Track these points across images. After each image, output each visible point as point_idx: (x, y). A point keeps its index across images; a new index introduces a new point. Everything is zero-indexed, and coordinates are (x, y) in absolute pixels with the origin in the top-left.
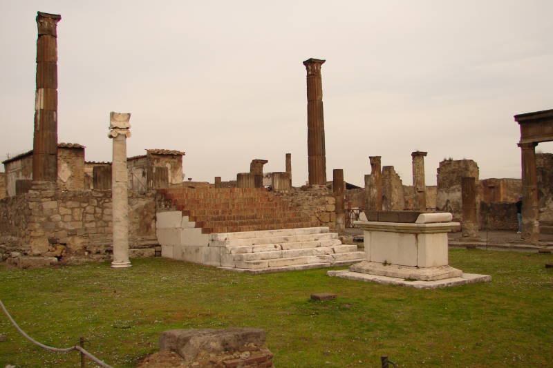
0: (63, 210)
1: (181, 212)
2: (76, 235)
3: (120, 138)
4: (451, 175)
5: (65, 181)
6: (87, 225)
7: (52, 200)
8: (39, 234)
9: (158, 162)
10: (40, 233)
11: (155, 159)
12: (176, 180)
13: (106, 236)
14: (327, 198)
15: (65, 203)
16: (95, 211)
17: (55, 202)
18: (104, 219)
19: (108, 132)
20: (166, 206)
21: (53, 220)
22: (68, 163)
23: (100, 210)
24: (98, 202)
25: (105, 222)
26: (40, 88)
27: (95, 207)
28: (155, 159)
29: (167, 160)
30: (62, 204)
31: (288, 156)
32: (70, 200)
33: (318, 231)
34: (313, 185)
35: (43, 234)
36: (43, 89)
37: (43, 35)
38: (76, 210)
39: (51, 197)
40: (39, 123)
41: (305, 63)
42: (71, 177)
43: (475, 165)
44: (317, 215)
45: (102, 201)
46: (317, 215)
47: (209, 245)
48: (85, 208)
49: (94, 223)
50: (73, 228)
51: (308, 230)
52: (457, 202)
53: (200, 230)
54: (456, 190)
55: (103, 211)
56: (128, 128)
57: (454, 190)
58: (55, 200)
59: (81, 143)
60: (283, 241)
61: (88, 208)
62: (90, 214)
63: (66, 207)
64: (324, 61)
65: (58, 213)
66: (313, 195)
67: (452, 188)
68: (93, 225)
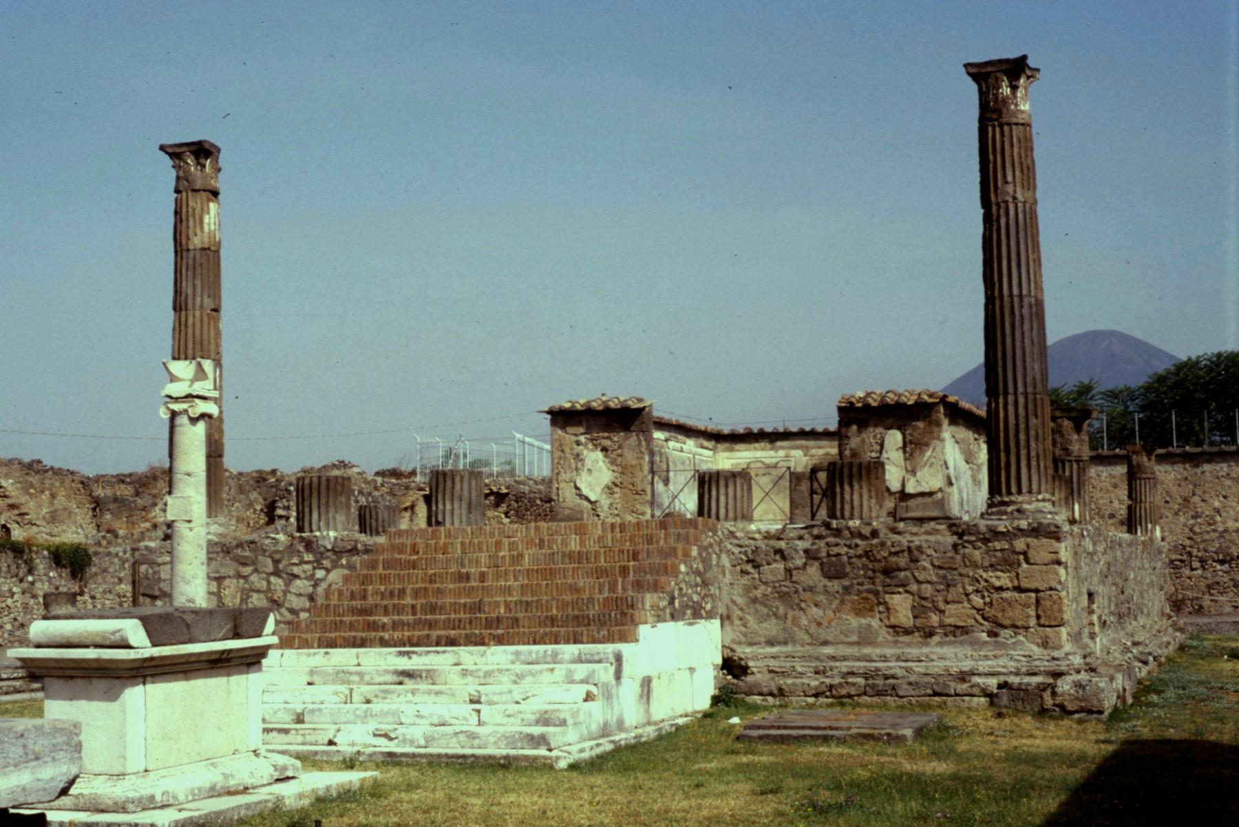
9: (860, 432)
14: (1020, 544)
16: (269, 582)
22: (604, 450)
23: (280, 581)
24: (276, 562)
33: (567, 657)
38: (227, 582)
42: (610, 489)
46: (977, 600)
60: (390, 678)
62: (258, 591)
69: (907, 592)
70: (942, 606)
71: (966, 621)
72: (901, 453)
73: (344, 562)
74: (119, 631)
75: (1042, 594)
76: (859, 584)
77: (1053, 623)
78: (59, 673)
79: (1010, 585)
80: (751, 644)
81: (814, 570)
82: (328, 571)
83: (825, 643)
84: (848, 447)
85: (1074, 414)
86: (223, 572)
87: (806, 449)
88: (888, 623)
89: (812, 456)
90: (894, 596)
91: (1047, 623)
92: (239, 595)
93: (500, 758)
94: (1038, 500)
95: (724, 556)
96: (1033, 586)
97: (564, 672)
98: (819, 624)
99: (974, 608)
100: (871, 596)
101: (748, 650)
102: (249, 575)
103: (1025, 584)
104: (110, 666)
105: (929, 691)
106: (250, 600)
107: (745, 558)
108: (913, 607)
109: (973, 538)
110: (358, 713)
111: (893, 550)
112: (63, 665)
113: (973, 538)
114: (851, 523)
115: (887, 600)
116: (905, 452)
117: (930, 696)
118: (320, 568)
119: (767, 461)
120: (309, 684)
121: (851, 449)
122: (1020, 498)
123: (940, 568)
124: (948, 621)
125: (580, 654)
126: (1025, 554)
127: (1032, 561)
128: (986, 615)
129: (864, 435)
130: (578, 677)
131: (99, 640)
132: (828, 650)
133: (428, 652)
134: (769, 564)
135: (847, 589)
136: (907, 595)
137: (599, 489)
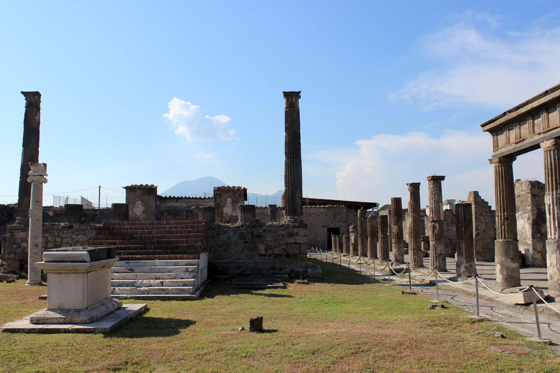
5: (139, 215)
7: (22, 231)
9: (220, 197)
11: (217, 194)
12: (236, 213)
14: (296, 230)
21: (22, 246)
24: (58, 233)
27: (55, 237)
29: (229, 195)
33: (183, 264)
35: (14, 257)
39: (21, 229)
42: (144, 212)
44: (284, 247)
45: (62, 232)
48: (47, 237)
51: (171, 262)
59: (155, 185)
61: (49, 238)
62: (51, 242)
69: (263, 244)
70: (273, 248)
71: (280, 252)
72: (231, 205)
73: (82, 232)
74: (82, 256)
75: (301, 245)
76: (249, 241)
77: (305, 253)
78: (56, 272)
79: (293, 242)
80: (217, 260)
81: (236, 237)
82: (77, 235)
83: (239, 259)
87: (187, 203)
88: (258, 253)
89: (188, 205)
90: (259, 245)
91: (303, 253)
93: (178, 298)
94: (300, 218)
95: (209, 232)
96: (299, 242)
97: (185, 269)
98: (238, 253)
99: (283, 248)
100: (253, 245)
101: (216, 261)
102: (48, 237)
103: (297, 242)
104: (78, 268)
105: (272, 273)
106: (48, 245)
107: (215, 233)
108: (265, 249)
109: (283, 228)
110: (120, 283)
111: (260, 231)
112: (58, 269)
113: (283, 228)
114: (247, 224)
115: (257, 246)
116: (232, 204)
117: (272, 274)
118: (74, 235)
119: (175, 206)
121: (217, 202)
122: (295, 217)
123: (273, 237)
124: (275, 252)
125: (187, 263)
126: (297, 233)
128: (286, 251)
129: (220, 199)
130: (190, 270)
131: (72, 259)
132: (241, 261)
133: (135, 262)
134: (222, 235)
135: (245, 242)
136: (263, 245)
137: (140, 212)
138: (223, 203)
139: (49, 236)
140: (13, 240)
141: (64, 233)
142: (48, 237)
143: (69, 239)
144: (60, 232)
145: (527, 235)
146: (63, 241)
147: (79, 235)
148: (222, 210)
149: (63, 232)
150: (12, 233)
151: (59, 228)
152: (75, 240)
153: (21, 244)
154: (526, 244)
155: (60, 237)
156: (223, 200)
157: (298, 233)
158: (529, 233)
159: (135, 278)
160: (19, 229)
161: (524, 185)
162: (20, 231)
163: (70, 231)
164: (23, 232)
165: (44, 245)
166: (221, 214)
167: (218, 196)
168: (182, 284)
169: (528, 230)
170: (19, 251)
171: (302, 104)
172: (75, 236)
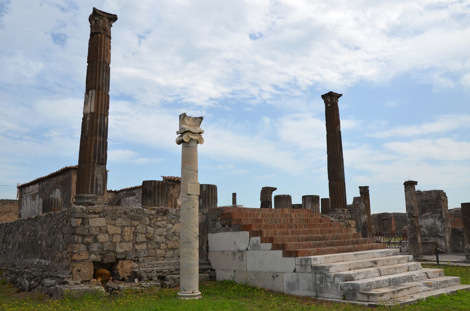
0: (111, 229)
1: (248, 232)
2: (124, 259)
3: (193, 144)
4: (423, 203)
6: (137, 247)
8: (83, 258)
9: (173, 188)
10: (84, 256)
11: (171, 185)
13: (157, 260)
14: (350, 221)
15: (115, 220)
16: (146, 229)
17: (103, 219)
18: (155, 240)
19: (176, 136)
20: (223, 226)
21: (100, 241)
25: (157, 243)
26: (92, 89)
28: (171, 185)
30: (110, 221)
31: (234, 195)
32: (120, 217)
33: (391, 254)
34: (336, 209)
35: (87, 258)
36: (94, 91)
37: (97, 33)
38: (126, 229)
39: (99, 213)
40: (88, 128)
41: (324, 97)
43: (444, 195)
45: (155, 220)
47: (295, 271)
48: (135, 227)
49: (145, 245)
50: (122, 251)
52: (430, 227)
53: (280, 252)
54: (429, 216)
55: (154, 231)
56: (200, 133)
57: (427, 217)
58: (104, 217)
61: (139, 227)
63: (115, 225)
64: (341, 95)
65: (107, 232)
66: (339, 218)
67: (424, 215)
68: (144, 246)
82: (173, 224)
84: (170, 193)
85: (272, 189)
86: (124, 223)
92: (132, 235)
102: (137, 225)
120: (350, 270)
121: (170, 194)
125: (394, 252)
126: (350, 225)
127: (352, 227)
130: (410, 260)
138: (176, 195)
139: (139, 225)
140: (87, 231)
141: (158, 221)
142: (137, 225)
143: (164, 230)
144: (152, 219)
145: (439, 229)
146: (156, 232)
147: (176, 223)
148: (176, 202)
149: (156, 219)
150: (83, 219)
151: (151, 213)
152: (172, 231)
153: (98, 237)
154: (437, 236)
155: (153, 225)
156: (176, 192)
157: (351, 225)
158: (441, 228)
159: (395, 271)
160: (95, 213)
161: (434, 193)
162: (97, 216)
163: (165, 218)
164: (101, 217)
165: (132, 237)
166: (174, 206)
167: (172, 186)
168: (438, 274)
169: (440, 226)
170: (95, 247)
171: (342, 105)
172: (171, 224)
